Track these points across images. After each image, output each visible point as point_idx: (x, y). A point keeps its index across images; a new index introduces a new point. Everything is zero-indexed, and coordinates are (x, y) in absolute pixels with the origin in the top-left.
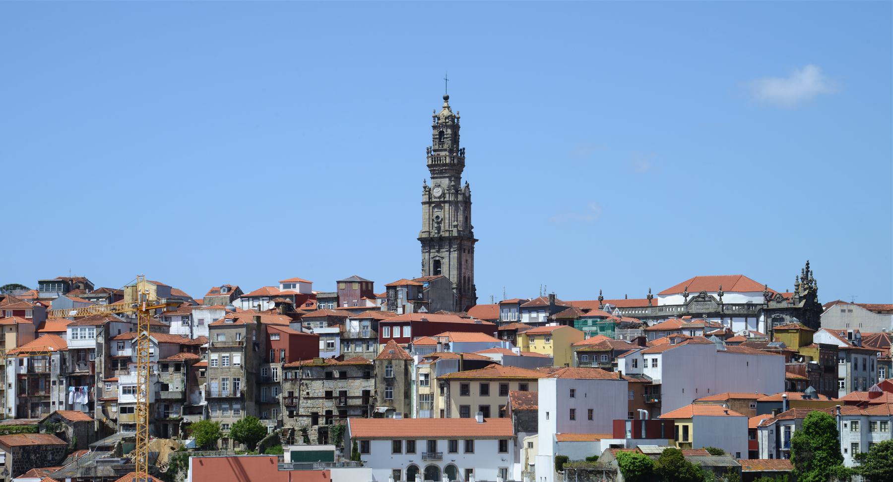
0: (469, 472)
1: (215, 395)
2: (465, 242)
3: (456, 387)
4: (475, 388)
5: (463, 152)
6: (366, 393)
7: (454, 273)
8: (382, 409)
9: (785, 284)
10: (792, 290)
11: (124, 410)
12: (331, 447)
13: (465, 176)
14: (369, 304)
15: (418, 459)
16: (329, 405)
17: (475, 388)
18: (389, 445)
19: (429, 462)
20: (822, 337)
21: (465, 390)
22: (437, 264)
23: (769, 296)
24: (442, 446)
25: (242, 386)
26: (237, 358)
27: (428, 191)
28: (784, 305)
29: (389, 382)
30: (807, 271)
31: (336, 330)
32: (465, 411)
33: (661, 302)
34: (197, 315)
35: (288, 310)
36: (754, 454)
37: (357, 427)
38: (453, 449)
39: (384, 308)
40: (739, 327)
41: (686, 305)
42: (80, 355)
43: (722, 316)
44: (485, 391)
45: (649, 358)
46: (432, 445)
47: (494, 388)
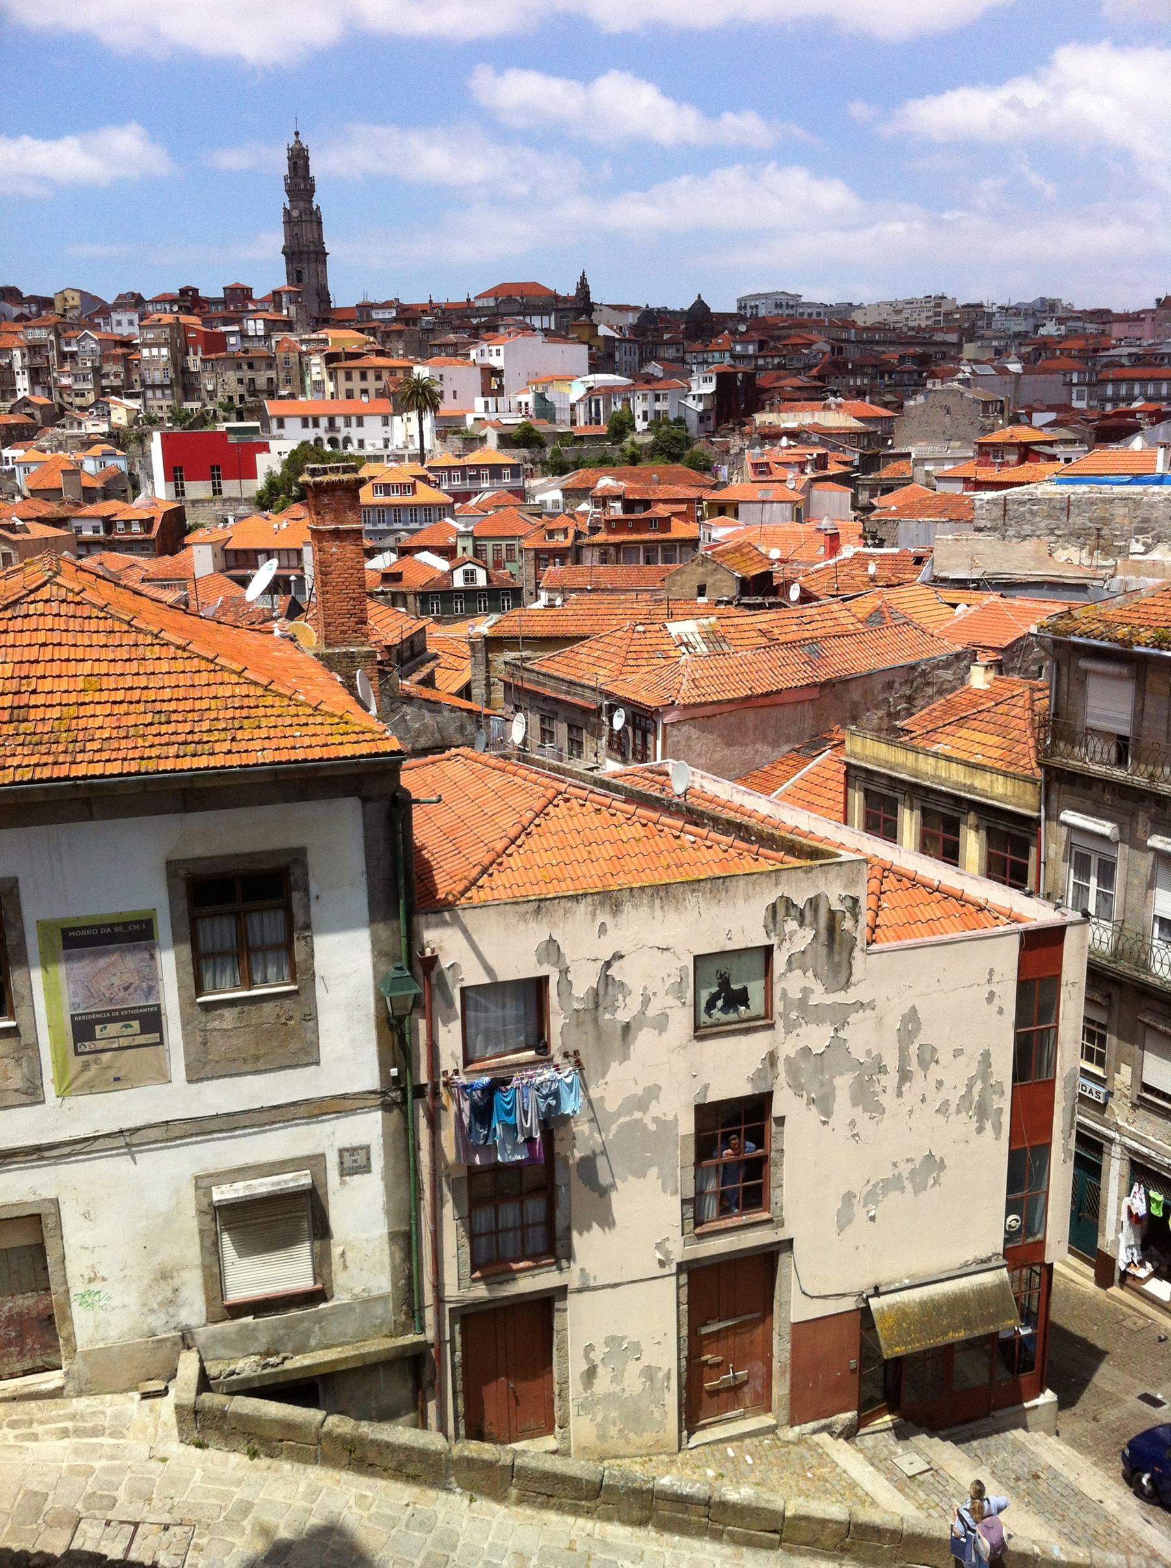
0: (361, 443)
1: (149, 382)
2: (320, 255)
3: (341, 375)
4: (356, 375)
5: (312, 179)
6: (270, 380)
7: (314, 280)
8: (283, 393)
9: (567, 289)
10: (573, 293)
11: (77, 395)
12: (258, 424)
13: (317, 200)
14: (251, 307)
15: (321, 432)
16: (241, 390)
17: (356, 375)
18: (299, 421)
19: (330, 435)
20: (603, 331)
21: (349, 377)
22: (299, 272)
23: (556, 297)
24: (339, 422)
25: (171, 374)
26: (164, 351)
27: (287, 213)
28: (569, 305)
29: (288, 370)
30: (583, 278)
31: (236, 328)
32: (350, 395)
33: (478, 304)
34: (115, 317)
35: (189, 311)
36: (573, 422)
37: (272, 407)
38: (348, 425)
39: (271, 310)
40: (536, 321)
41: (497, 306)
42: (34, 349)
43: (524, 315)
44: (364, 377)
45: (494, 348)
46: (331, 421)
47: (371, 375)
